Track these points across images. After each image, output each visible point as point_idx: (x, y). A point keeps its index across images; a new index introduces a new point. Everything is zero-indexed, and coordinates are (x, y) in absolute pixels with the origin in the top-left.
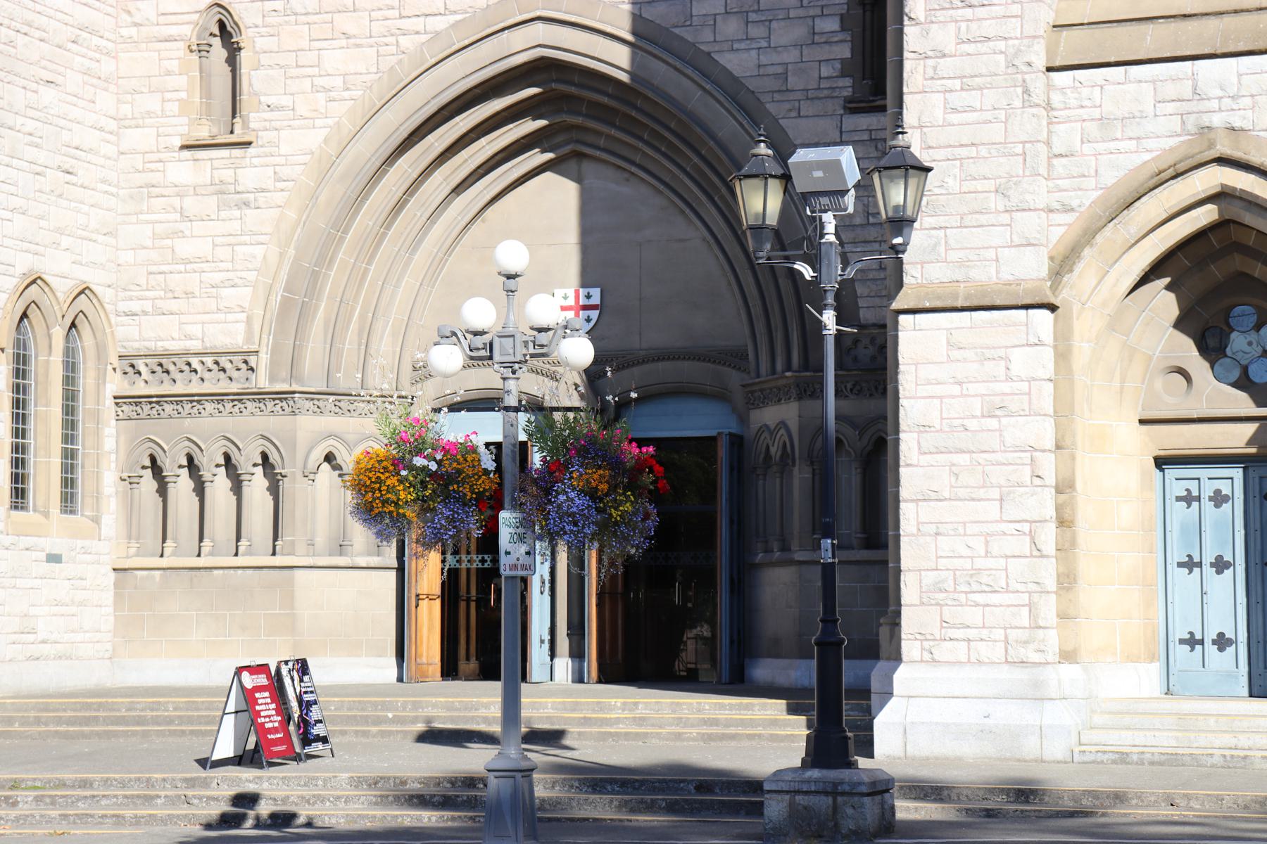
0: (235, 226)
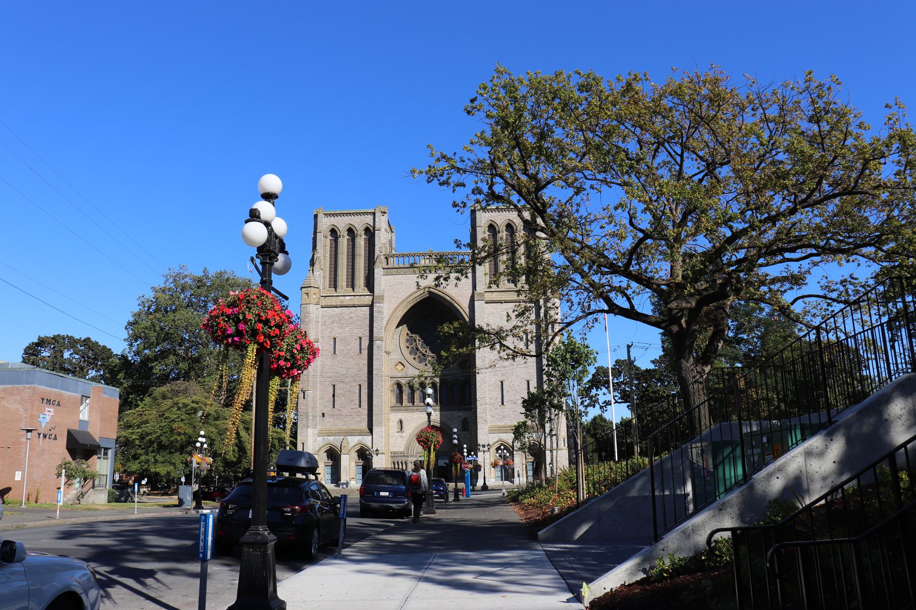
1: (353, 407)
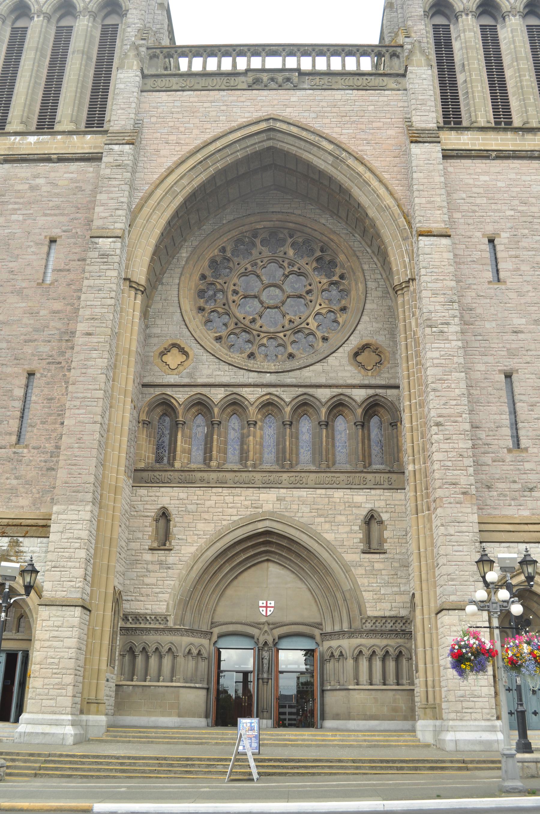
0: (165, 575)
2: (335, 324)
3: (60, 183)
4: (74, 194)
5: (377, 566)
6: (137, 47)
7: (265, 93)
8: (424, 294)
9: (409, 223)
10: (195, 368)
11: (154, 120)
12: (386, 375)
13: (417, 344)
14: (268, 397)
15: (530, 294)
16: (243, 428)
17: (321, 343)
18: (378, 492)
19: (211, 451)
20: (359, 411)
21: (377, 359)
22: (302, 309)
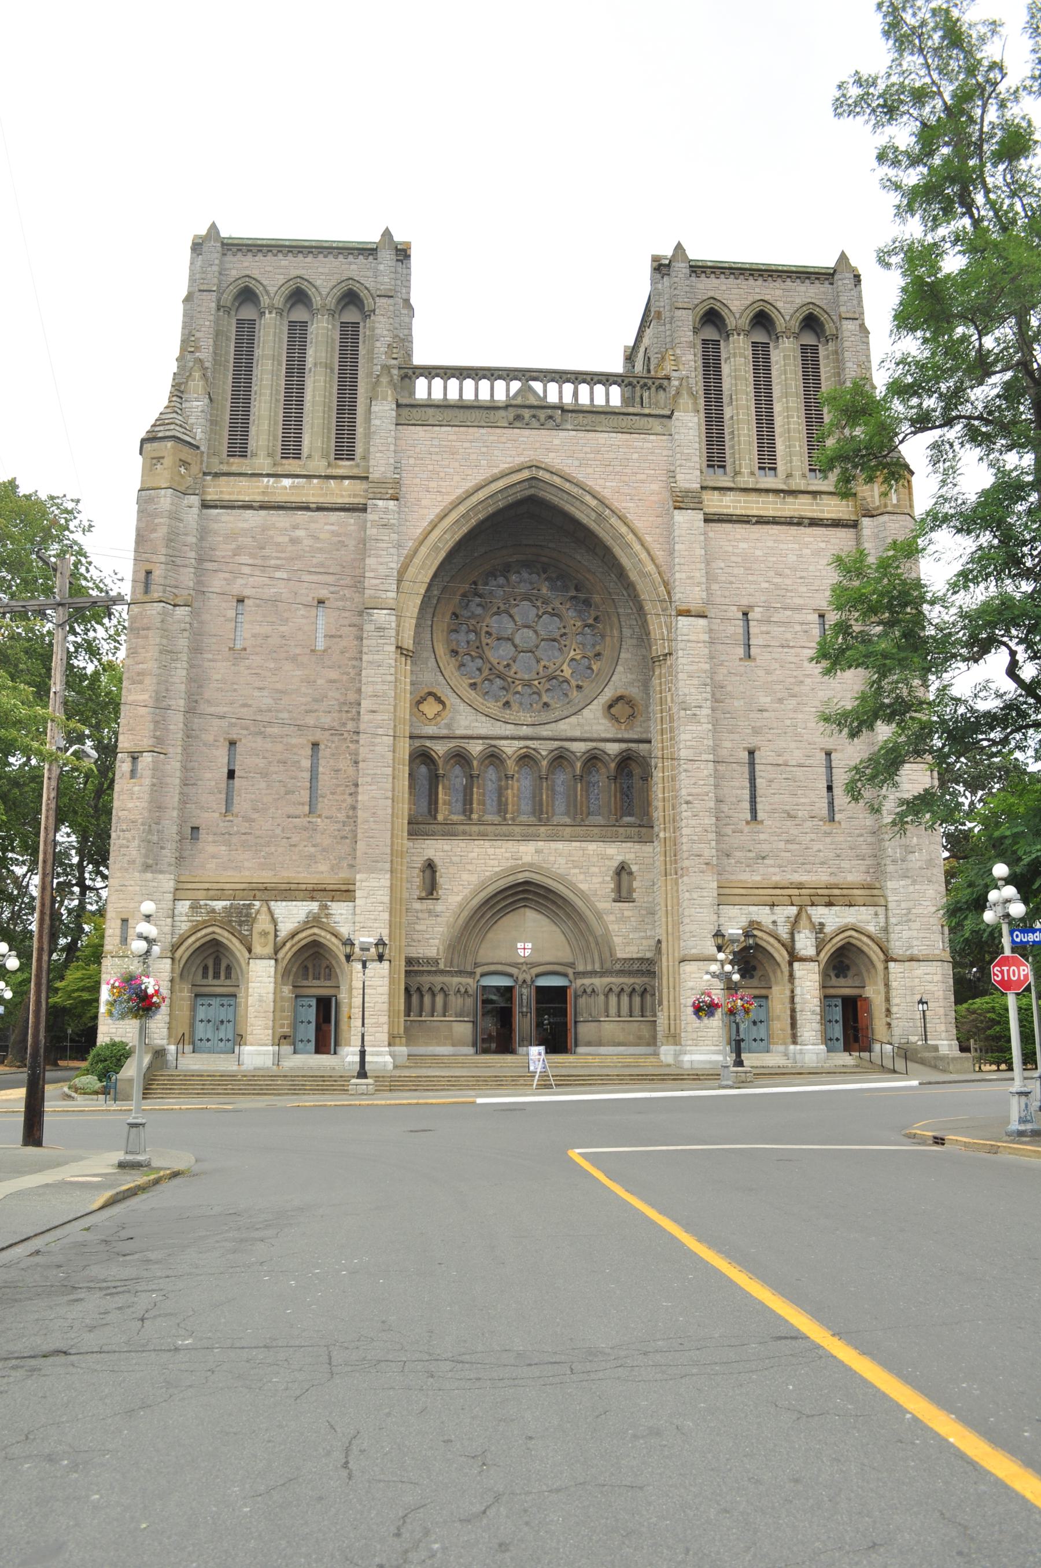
1: (292, 810)
2: (589, 671)
3: (322, 536)
4: (338, 550)
5: (626, 913)
6: (386, 368)
7: (527, 432)
8: (681, 676)
9: (669, 593)
10: (452, 719)
11: (412, 461)
12: (639, 729)
13: (672, 720)
14: (525, 750)
15: (777, 672)
16: (500, 780)
17: (575, 693)
18: (629, 845)
19: (471, 804)
20: (613, 765)
21: (630, 711)
22: (557, 653)
